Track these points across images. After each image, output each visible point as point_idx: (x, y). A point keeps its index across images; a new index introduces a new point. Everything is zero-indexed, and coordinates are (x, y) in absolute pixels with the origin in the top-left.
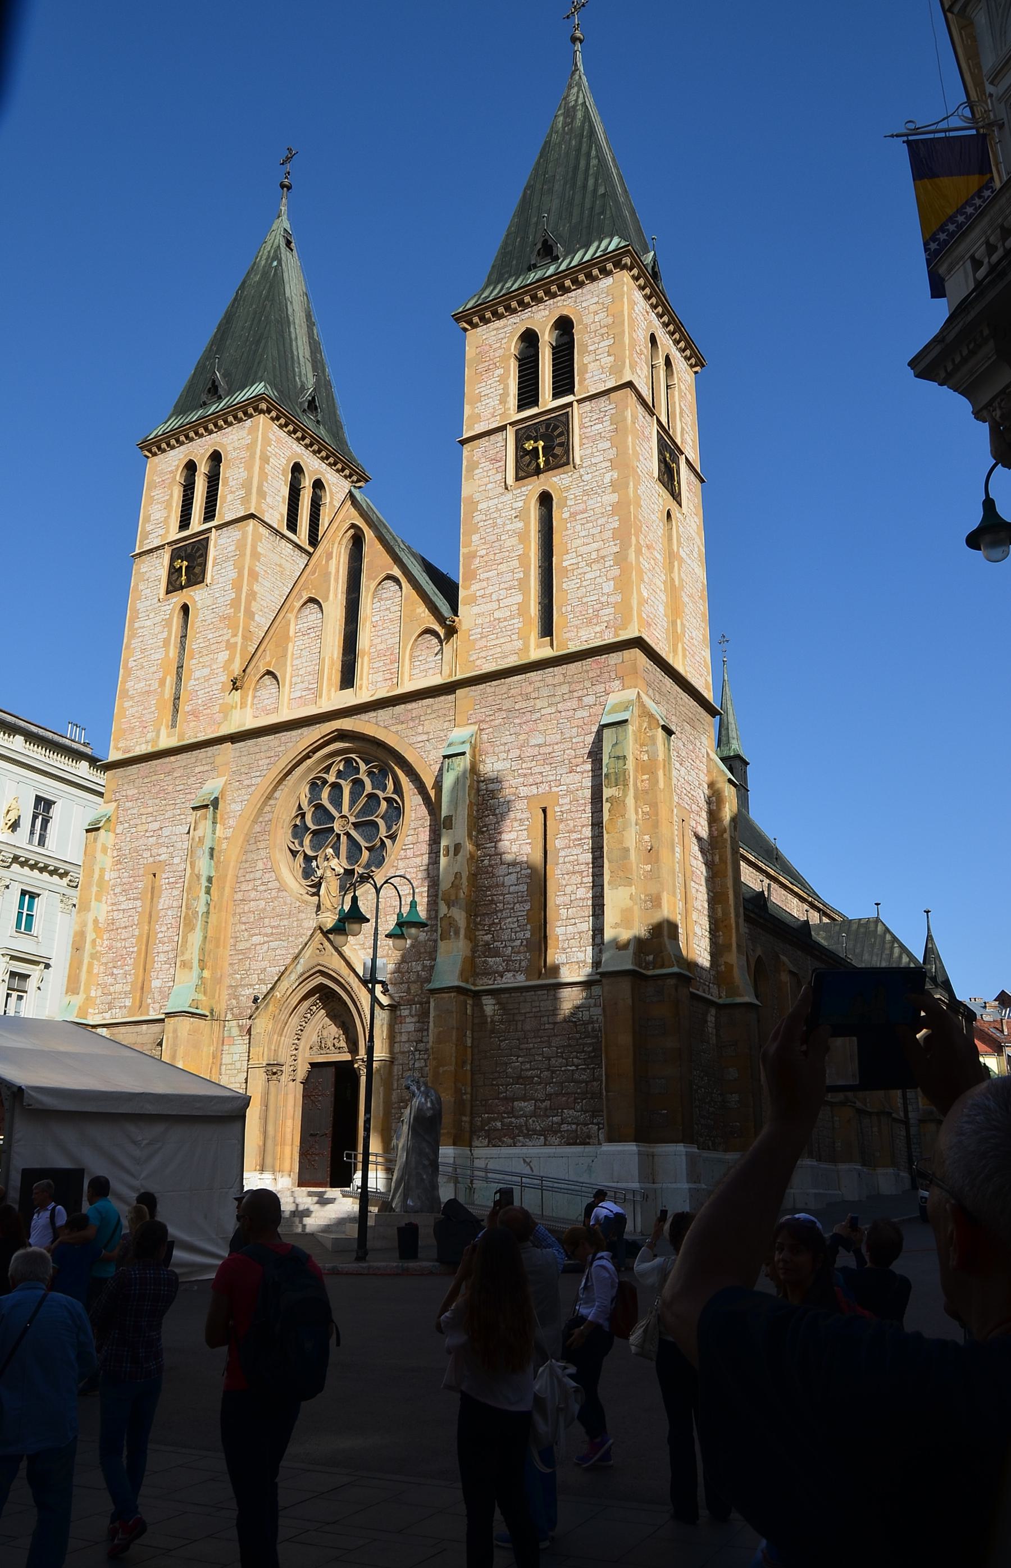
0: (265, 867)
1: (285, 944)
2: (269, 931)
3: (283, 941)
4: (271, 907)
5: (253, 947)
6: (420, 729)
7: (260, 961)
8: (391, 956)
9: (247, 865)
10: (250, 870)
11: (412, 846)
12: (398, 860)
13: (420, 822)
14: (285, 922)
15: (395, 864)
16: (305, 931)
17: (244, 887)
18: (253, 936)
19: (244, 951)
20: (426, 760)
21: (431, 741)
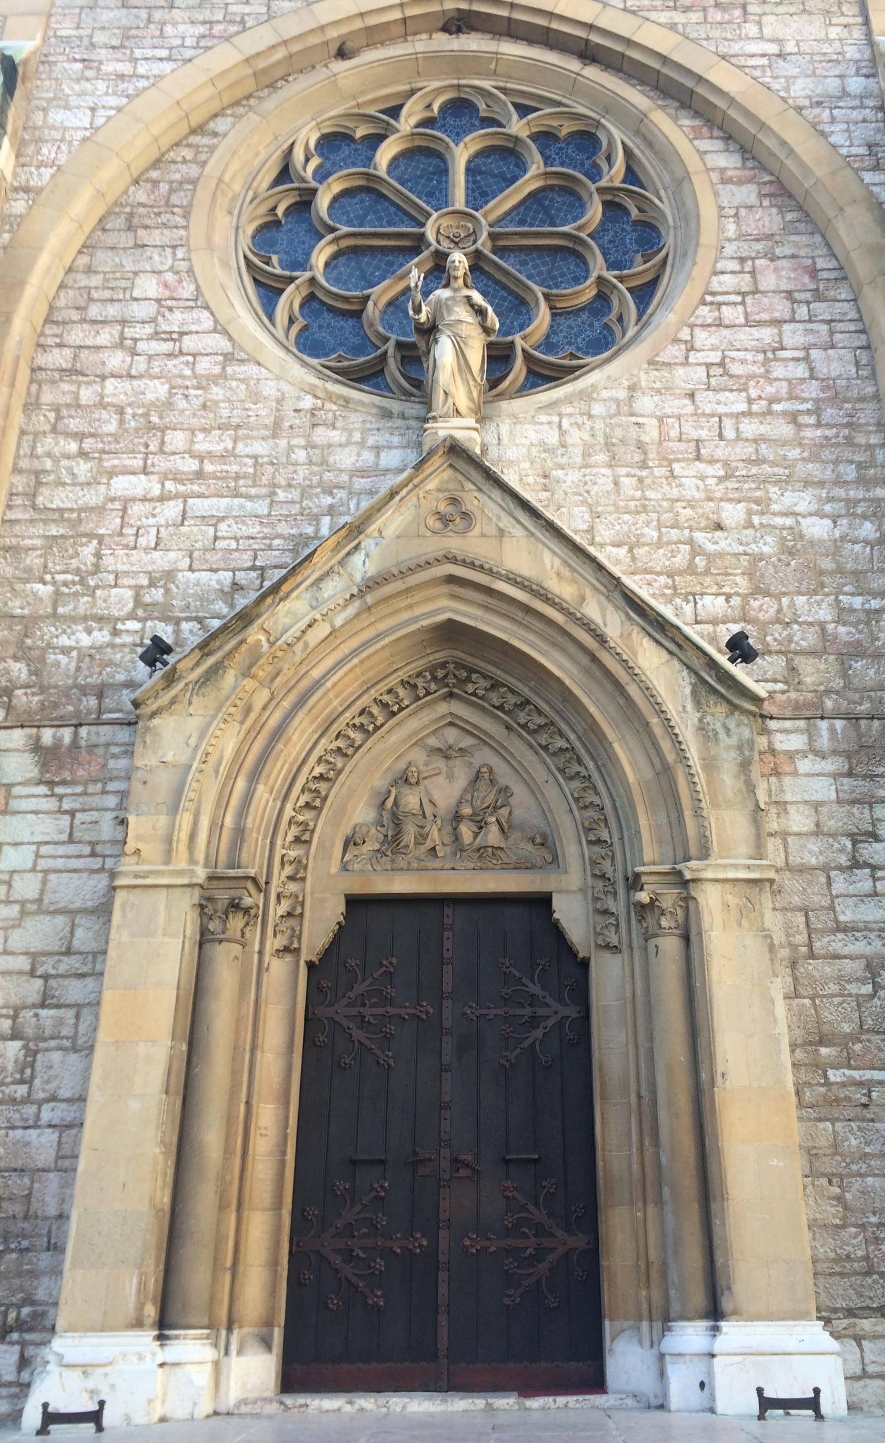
0: (167, 294)
1: (262, 507)
2: (190, 465)
3: (248, 497)
4: (197, 402)
5: (117, 505)
6: (751, 29)
7: (146, 550)
8: (707, 572)
9: (96, 280)
10: (107, 294)
11: (739, 299)
12: (692, 326)
13: (759, 246)
14: (260, 448)
15: (685, 334)
16: (345, 477)
17: (77, 335)
18: (112, 474)
19: (75, 515)
20: (782, 94)
21: (788, 58)
